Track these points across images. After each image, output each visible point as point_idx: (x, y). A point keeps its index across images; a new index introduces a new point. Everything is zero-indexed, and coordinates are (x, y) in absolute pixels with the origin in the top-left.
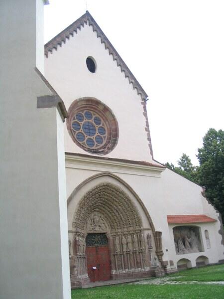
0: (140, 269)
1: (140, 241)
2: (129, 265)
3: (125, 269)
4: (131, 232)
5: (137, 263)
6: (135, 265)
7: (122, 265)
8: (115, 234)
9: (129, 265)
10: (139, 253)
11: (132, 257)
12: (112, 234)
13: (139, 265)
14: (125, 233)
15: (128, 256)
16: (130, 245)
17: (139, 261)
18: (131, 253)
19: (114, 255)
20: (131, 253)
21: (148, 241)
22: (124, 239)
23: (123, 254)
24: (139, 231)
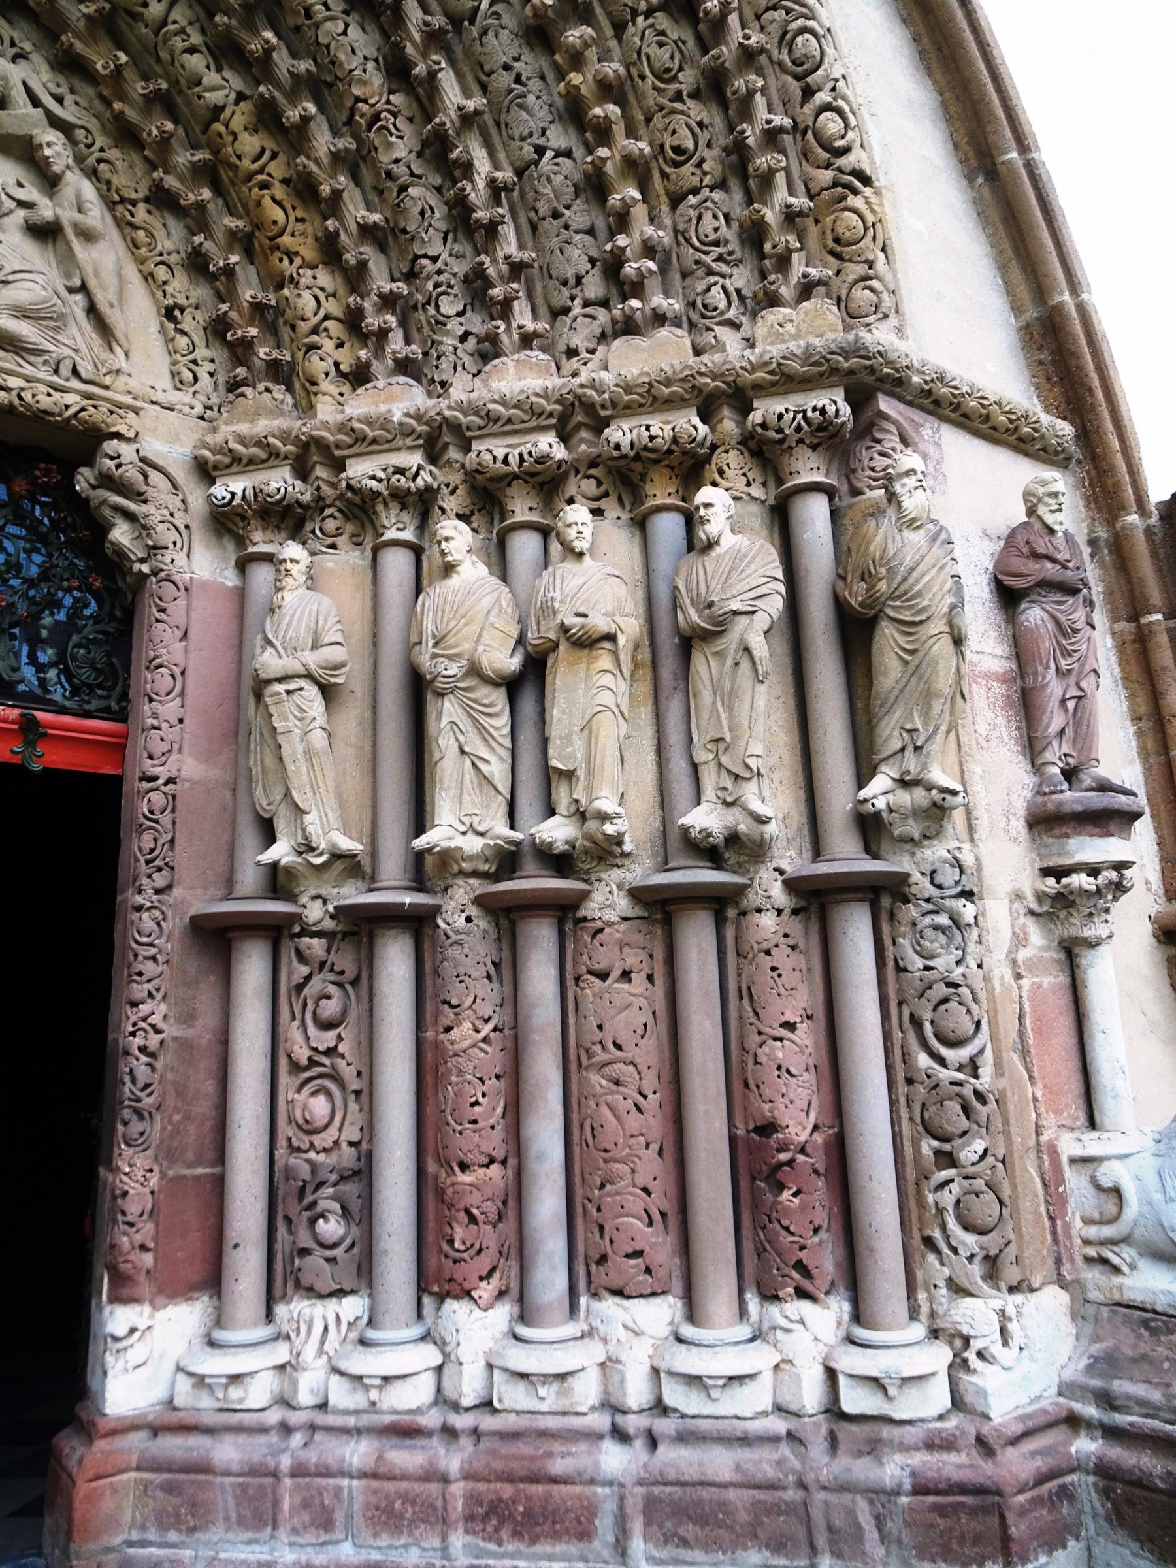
0: (814, 1326)
1: (856, 629)
2: (547, 1205)
3: (437, 1282)
4: (623, 433)
5: (757, 1157)
6: (681, 1217)
7: (364, 1171)
8: (279, 481)
9: (547, 1205)
10: (816, 899)
11: (626, 1008)
12: (234, 487)
13: (803, 1205)
14: (493, 451)
15: (541, 976)
16: (596, 706)
17: (798, 1117)
18: (608, 900)
19: (217, 938)
20: (608, 900)
21: (1021, 652)
22: (473, 572)
23: (419, 924)
24: (834, 402)
